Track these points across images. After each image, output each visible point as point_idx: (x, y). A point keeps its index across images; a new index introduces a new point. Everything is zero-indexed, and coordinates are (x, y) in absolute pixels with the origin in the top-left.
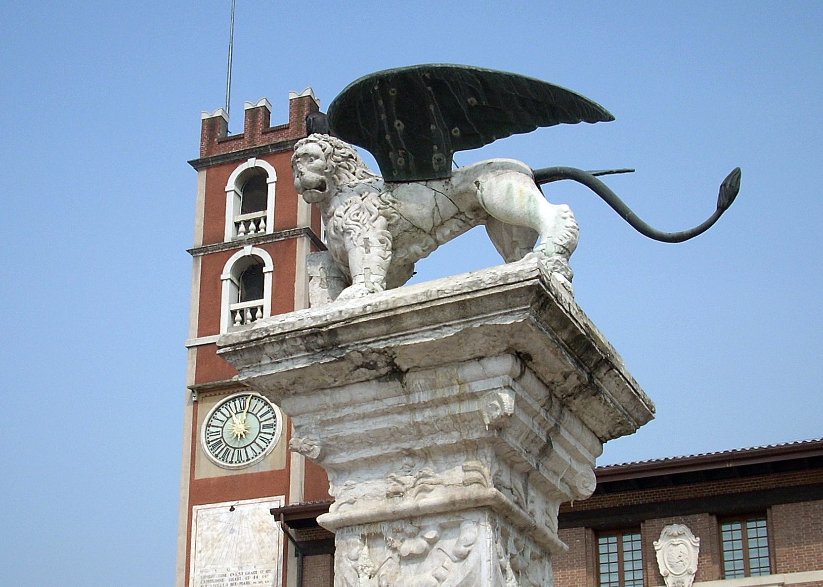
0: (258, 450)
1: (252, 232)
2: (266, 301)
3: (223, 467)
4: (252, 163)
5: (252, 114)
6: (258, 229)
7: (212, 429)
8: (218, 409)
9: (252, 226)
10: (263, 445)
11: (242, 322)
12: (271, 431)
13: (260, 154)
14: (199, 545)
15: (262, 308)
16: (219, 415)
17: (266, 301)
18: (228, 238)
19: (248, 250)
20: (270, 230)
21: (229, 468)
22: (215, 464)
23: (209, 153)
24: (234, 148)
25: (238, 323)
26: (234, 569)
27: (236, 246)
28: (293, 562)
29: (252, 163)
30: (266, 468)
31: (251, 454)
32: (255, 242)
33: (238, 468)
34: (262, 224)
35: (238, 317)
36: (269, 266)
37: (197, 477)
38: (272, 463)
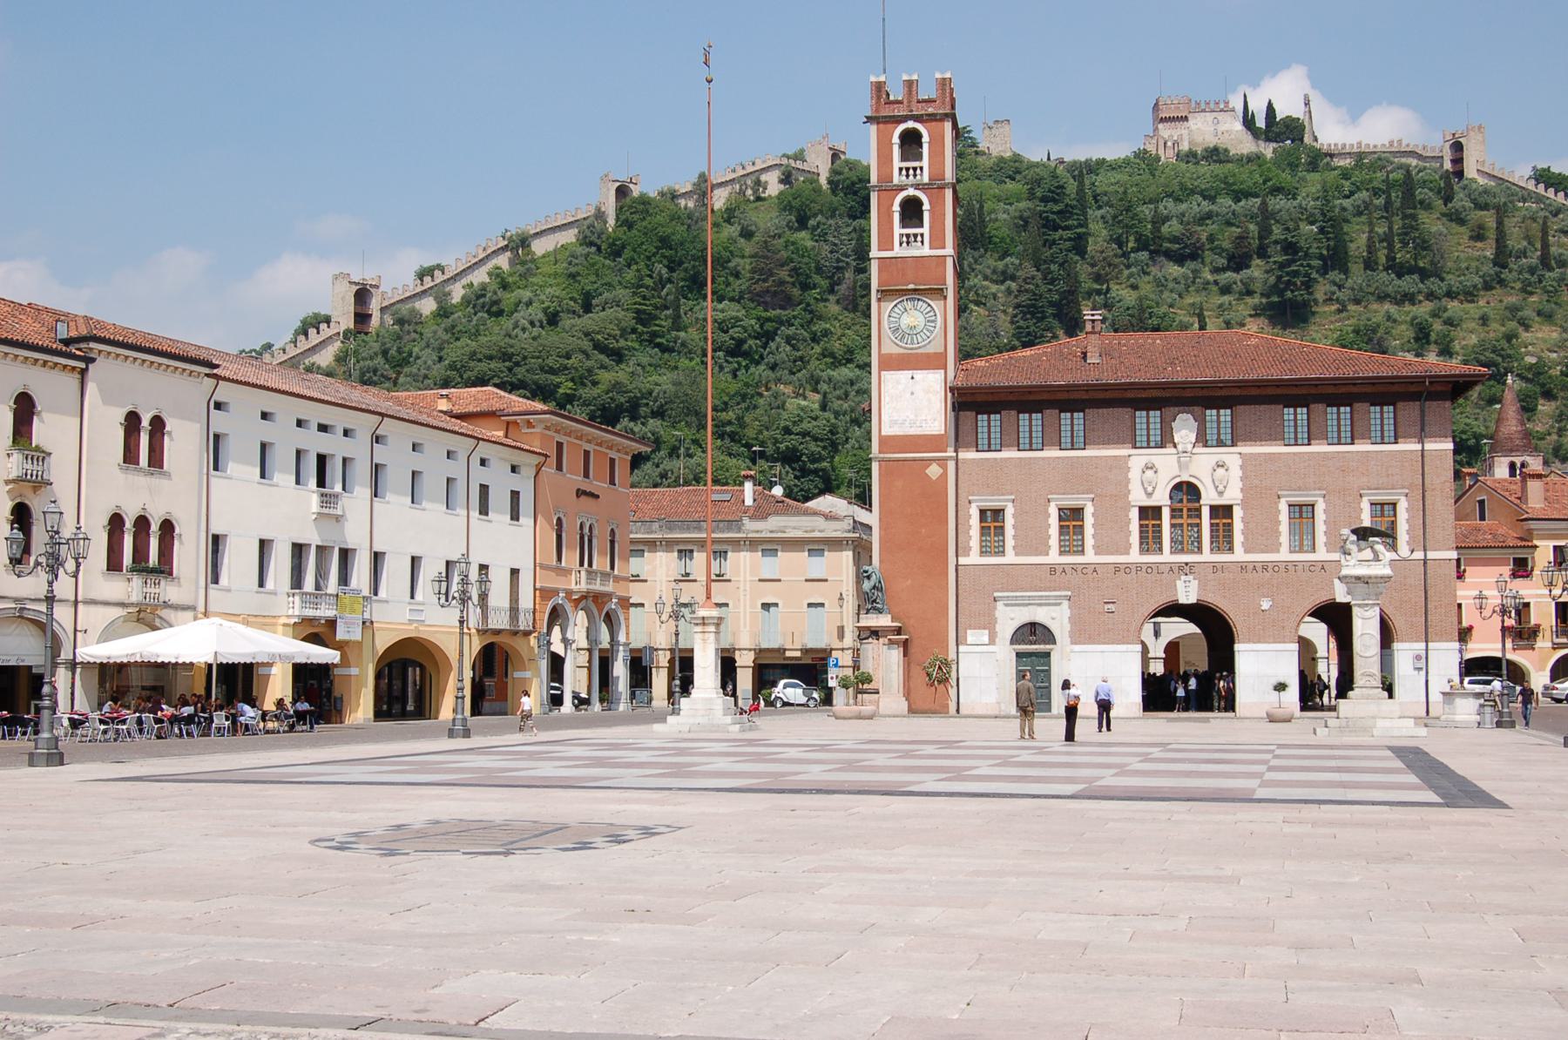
0: (925, 337)
1: (911, 177)
2: (926, 230)
3: (901, 347)
4: (910, 124)
5: (910, 84)
6: (915, 175)
7: (891, 319)
8: (896, 306)
9: (911, 172)
10: (928, 334)
11: (908, 243)
12: (933, 324)
13: (917, 119)
14: (887, 399)
15: (922, 235)
16: (896, 310)
17: (926, 230)
18: (896, 180)
19: (911, 192)
20: (926, 179)
21: (906, 348)
22: (897, 345)
23: (877, 111)
24: (900, 111)
25: (904, 245)
26: (912, 417)
27: (902, 188)
29: (910, 124)
30: (930, 349)
31: (920, 340)
32: (917, 187)
33: (912, 349)
34: (918, 171)
35: (905, 239)
36: (926, 206)
37: (883, 352)
38: (935, 347)
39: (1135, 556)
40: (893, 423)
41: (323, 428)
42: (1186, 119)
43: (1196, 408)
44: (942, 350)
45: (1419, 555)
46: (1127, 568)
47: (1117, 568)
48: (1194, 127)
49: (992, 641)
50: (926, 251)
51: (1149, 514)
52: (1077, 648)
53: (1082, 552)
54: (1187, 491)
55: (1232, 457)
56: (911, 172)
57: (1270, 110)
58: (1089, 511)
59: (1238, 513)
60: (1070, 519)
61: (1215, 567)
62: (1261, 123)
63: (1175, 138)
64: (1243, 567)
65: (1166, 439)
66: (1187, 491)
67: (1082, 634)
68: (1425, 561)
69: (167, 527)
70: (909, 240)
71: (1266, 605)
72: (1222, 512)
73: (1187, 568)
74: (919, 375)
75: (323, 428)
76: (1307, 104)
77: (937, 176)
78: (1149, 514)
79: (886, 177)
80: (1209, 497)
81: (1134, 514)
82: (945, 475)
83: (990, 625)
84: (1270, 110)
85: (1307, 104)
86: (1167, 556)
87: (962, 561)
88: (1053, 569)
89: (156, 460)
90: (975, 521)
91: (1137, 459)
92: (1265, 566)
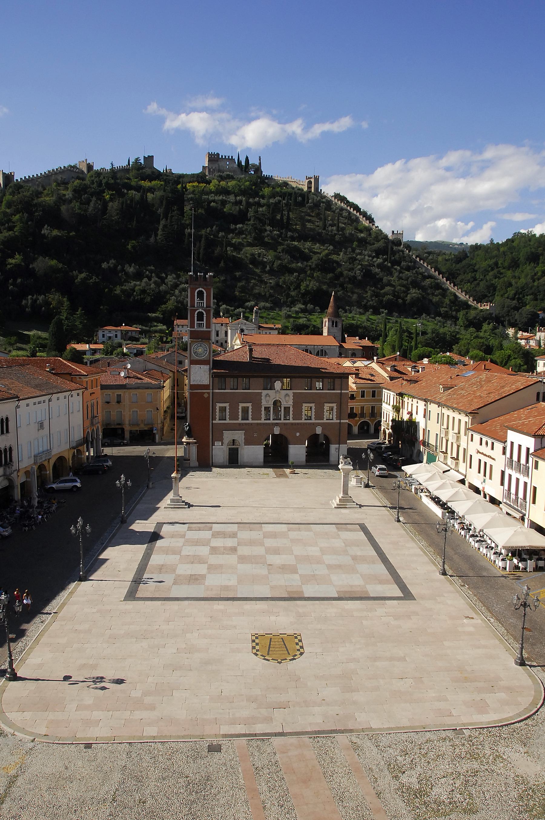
9: (200, 304)
15: (203, 324)
18: (196, 306)
19: (200, 310)
20: (205, 306)
28: (211, 379)
29: (201, 289)
36: (205, 315)
39: (263, 421)
40: (194, 381)
41: (40, 403)
42: (217, 161)
43: (281, 379)
44: (209, 359)
45: (339, 421)
46: (260, 424)
47: (258, 424)
48: (220, 165)
49: (222, 445)
50: (205, 329)
51: (267, 409)
52: (246, 446)
53: (248, 420)
54: (276, 403)
55: (291, 393)
56: (200, 304)
57: (247, 160)
58: (250, 408)
59: (291, 409)
60: (245, 411)
61: (285, 424)
62: (243, 164)
63: (214, 168)
64: (292, 424)
65: (272, 388)
66: (276, 403)
67: (248, 442)
68: (340, 423)
69: (10, 448)
70: (200, 325)
71: (298, 434)
72: (287, 409)
73: (277, 424)
74: (202, 366)
75: (40, 403)
76: (260, 160)
77: (208, 306)
78: (267, 409)
79: (193, 305)
80: (284, 404)
81: (263, 409)
82: (209, 397)
83: (221, 440)
84: (247, 160)
85: (260, 160)
86: (271, 421)
87: (214, 422)
88: (240, 424)
89: (7, 431)
90: (217, 410)
91: (265, 392)
92: (298, 424)
